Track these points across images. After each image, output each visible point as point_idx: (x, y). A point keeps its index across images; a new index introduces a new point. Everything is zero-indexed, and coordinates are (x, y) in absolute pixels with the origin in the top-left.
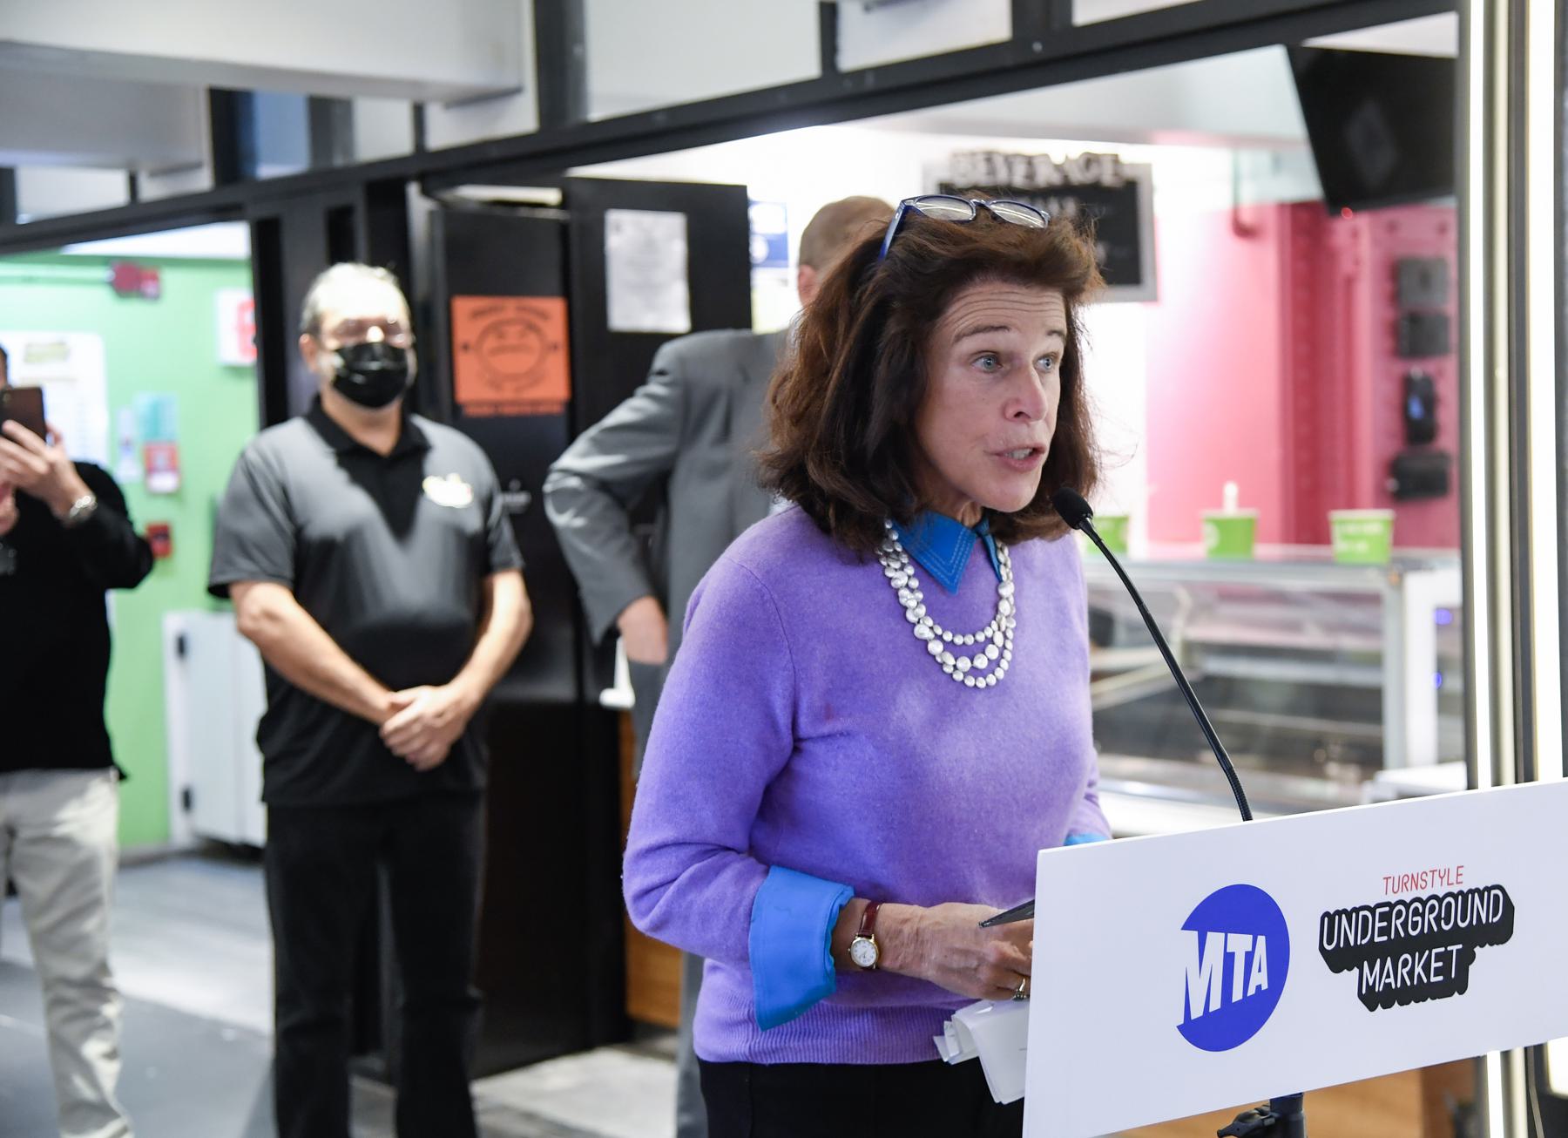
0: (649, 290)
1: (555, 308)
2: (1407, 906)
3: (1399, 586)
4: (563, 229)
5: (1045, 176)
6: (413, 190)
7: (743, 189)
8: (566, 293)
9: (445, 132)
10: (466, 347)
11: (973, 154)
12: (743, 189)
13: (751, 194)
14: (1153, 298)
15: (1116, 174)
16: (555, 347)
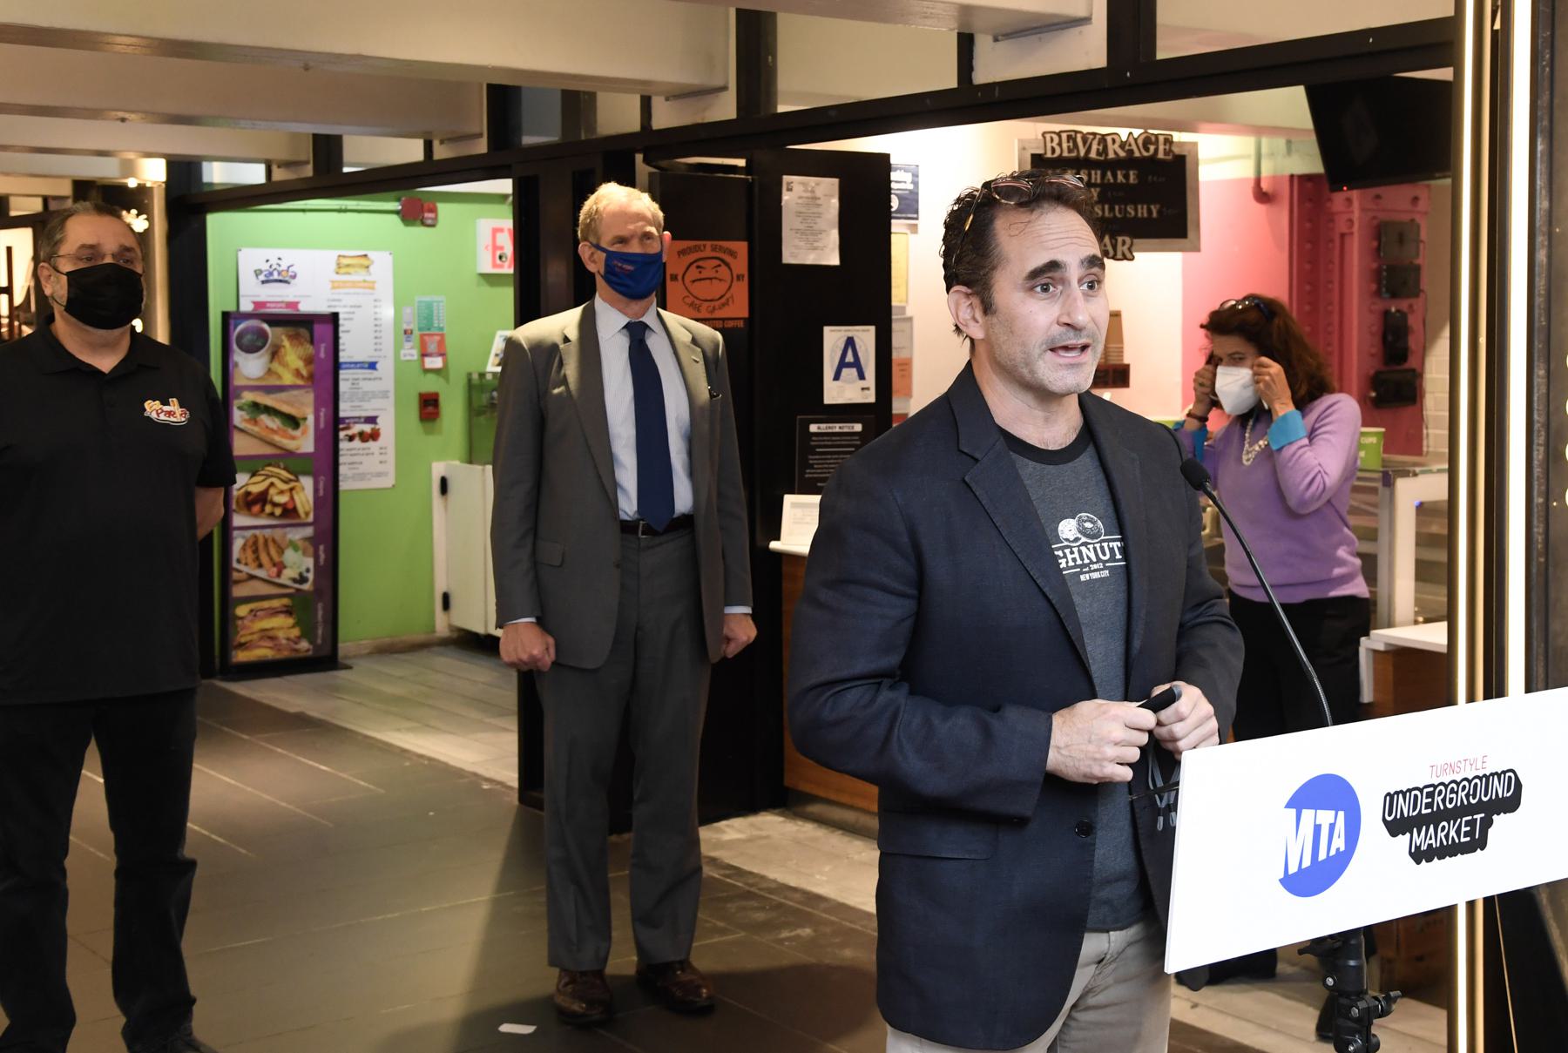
0: (812, 235)
1: (741, 247)
2: (1446, 786)
3: (1388, 480)
4: (749, 186)
5: (1113, 151)
6: (639, 157)
7: (887, 157)
8: (750, 239)
9: (666, 117)
10: (674, 278)
11: (1059, 134)
12: (887, 157)
13: (893, 161)
14: (1198, 249)
15: (1166, 153)
16: (739, 277)
